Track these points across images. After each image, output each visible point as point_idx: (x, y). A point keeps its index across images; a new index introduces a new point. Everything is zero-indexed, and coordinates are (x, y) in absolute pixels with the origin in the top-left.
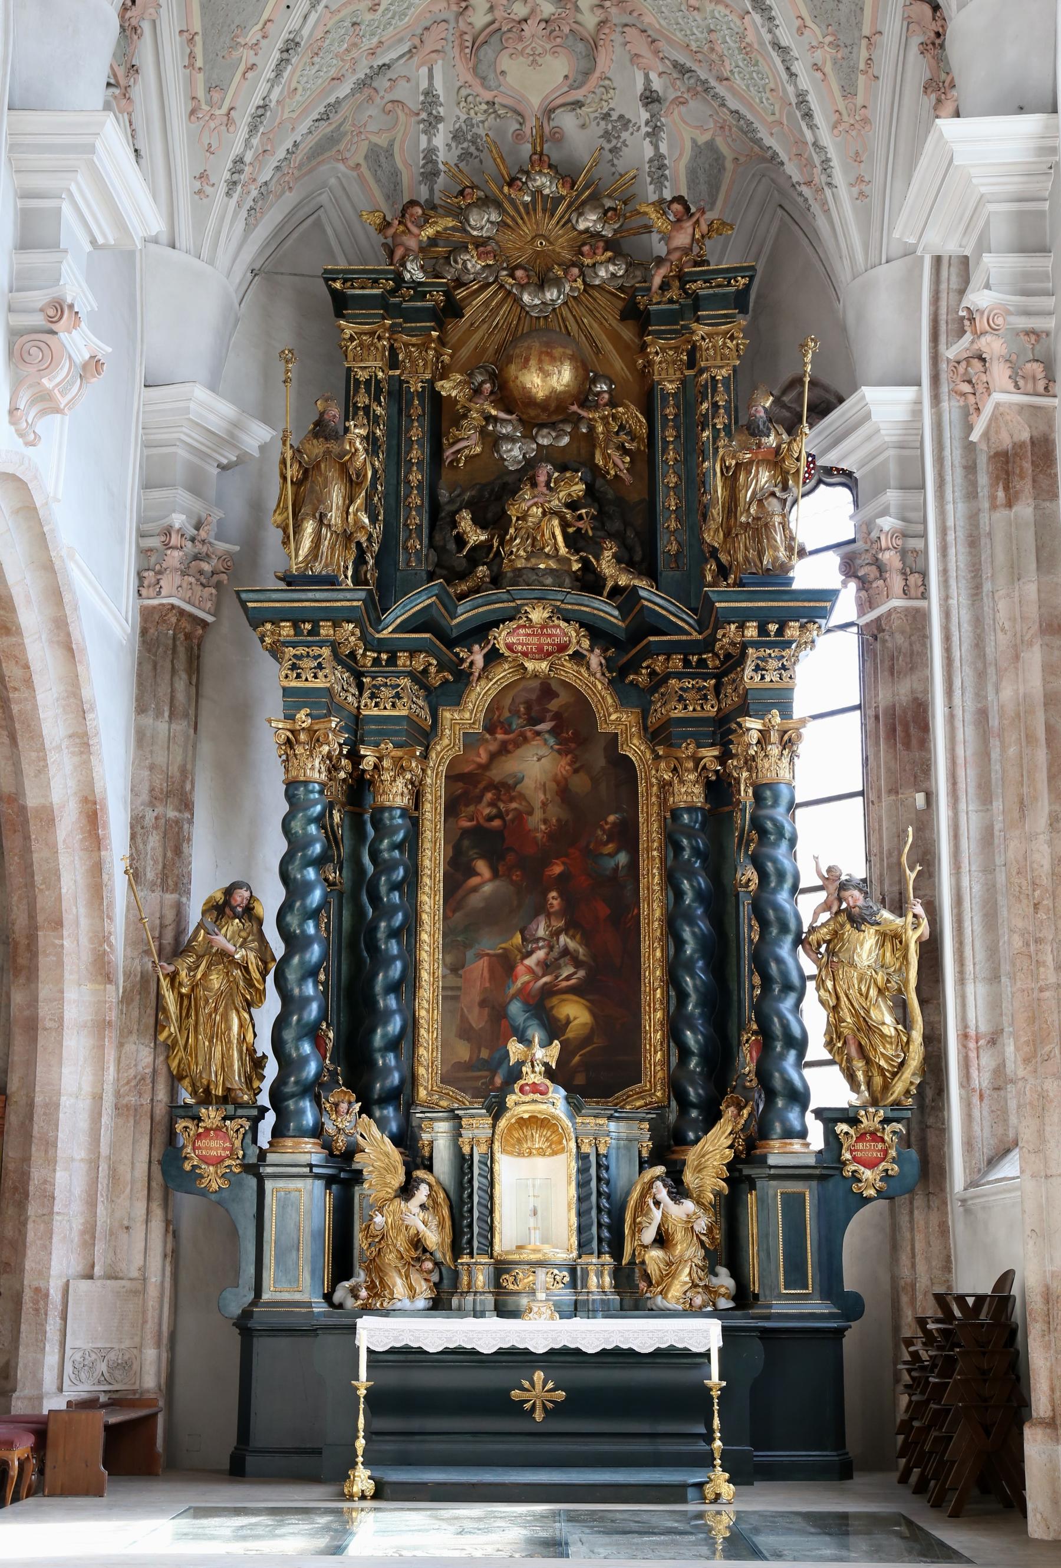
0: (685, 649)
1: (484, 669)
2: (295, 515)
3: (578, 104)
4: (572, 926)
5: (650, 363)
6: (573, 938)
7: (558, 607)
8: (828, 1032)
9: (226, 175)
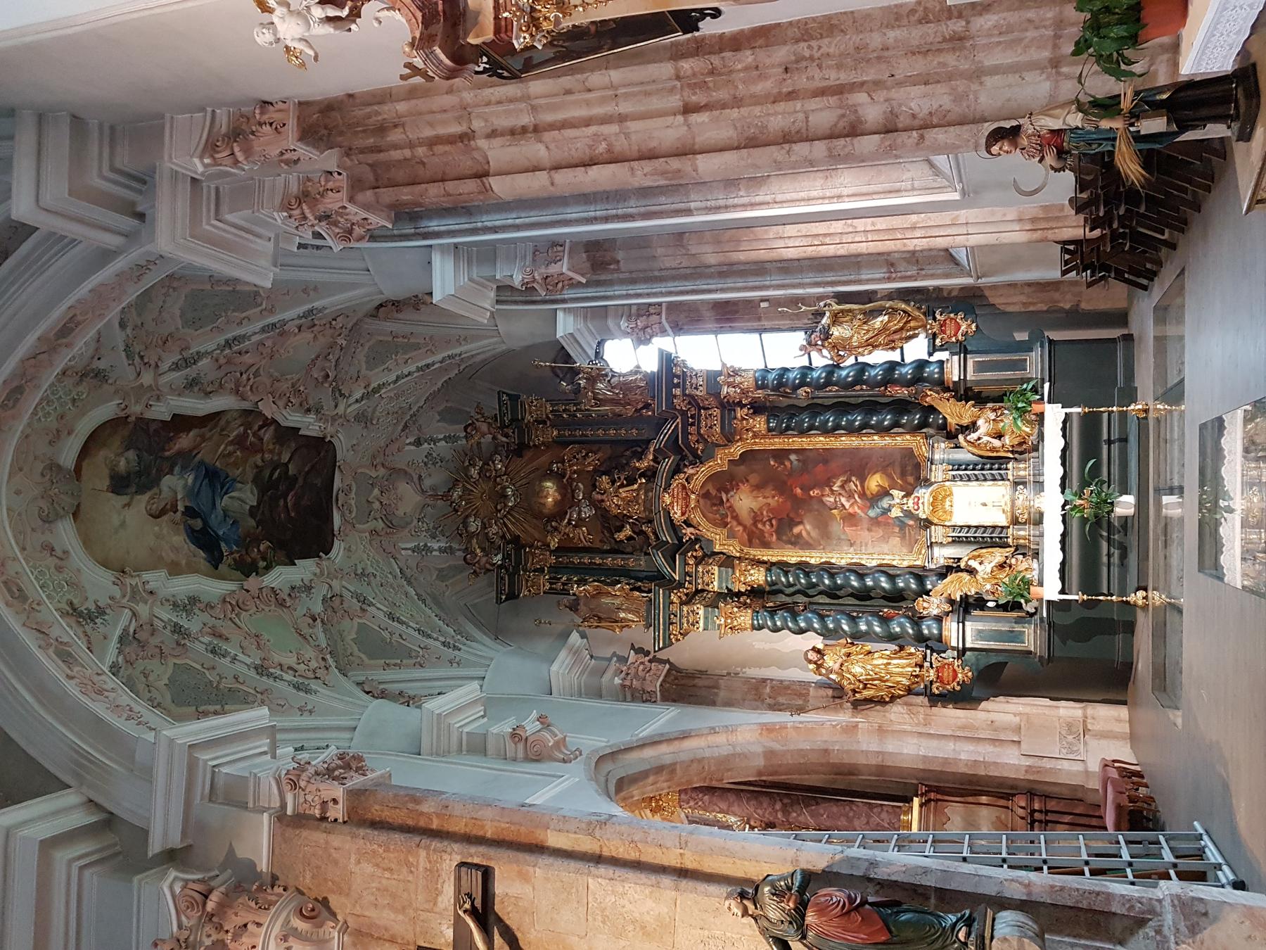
0: (686, 425)
1: (694, 527)
2: (617, 622)
3: (420, 476)
4: (828, 483)
5: (543, 443)
6: (835, 483)
7: (664, 489)
8: (887, 349)
9: (450, 650)
